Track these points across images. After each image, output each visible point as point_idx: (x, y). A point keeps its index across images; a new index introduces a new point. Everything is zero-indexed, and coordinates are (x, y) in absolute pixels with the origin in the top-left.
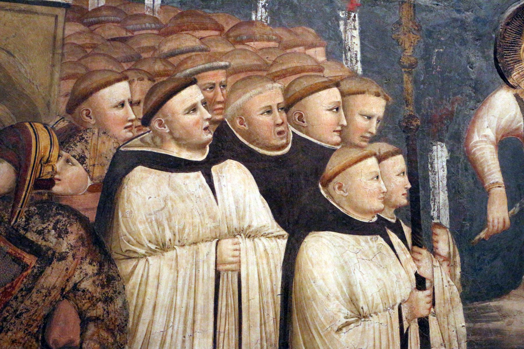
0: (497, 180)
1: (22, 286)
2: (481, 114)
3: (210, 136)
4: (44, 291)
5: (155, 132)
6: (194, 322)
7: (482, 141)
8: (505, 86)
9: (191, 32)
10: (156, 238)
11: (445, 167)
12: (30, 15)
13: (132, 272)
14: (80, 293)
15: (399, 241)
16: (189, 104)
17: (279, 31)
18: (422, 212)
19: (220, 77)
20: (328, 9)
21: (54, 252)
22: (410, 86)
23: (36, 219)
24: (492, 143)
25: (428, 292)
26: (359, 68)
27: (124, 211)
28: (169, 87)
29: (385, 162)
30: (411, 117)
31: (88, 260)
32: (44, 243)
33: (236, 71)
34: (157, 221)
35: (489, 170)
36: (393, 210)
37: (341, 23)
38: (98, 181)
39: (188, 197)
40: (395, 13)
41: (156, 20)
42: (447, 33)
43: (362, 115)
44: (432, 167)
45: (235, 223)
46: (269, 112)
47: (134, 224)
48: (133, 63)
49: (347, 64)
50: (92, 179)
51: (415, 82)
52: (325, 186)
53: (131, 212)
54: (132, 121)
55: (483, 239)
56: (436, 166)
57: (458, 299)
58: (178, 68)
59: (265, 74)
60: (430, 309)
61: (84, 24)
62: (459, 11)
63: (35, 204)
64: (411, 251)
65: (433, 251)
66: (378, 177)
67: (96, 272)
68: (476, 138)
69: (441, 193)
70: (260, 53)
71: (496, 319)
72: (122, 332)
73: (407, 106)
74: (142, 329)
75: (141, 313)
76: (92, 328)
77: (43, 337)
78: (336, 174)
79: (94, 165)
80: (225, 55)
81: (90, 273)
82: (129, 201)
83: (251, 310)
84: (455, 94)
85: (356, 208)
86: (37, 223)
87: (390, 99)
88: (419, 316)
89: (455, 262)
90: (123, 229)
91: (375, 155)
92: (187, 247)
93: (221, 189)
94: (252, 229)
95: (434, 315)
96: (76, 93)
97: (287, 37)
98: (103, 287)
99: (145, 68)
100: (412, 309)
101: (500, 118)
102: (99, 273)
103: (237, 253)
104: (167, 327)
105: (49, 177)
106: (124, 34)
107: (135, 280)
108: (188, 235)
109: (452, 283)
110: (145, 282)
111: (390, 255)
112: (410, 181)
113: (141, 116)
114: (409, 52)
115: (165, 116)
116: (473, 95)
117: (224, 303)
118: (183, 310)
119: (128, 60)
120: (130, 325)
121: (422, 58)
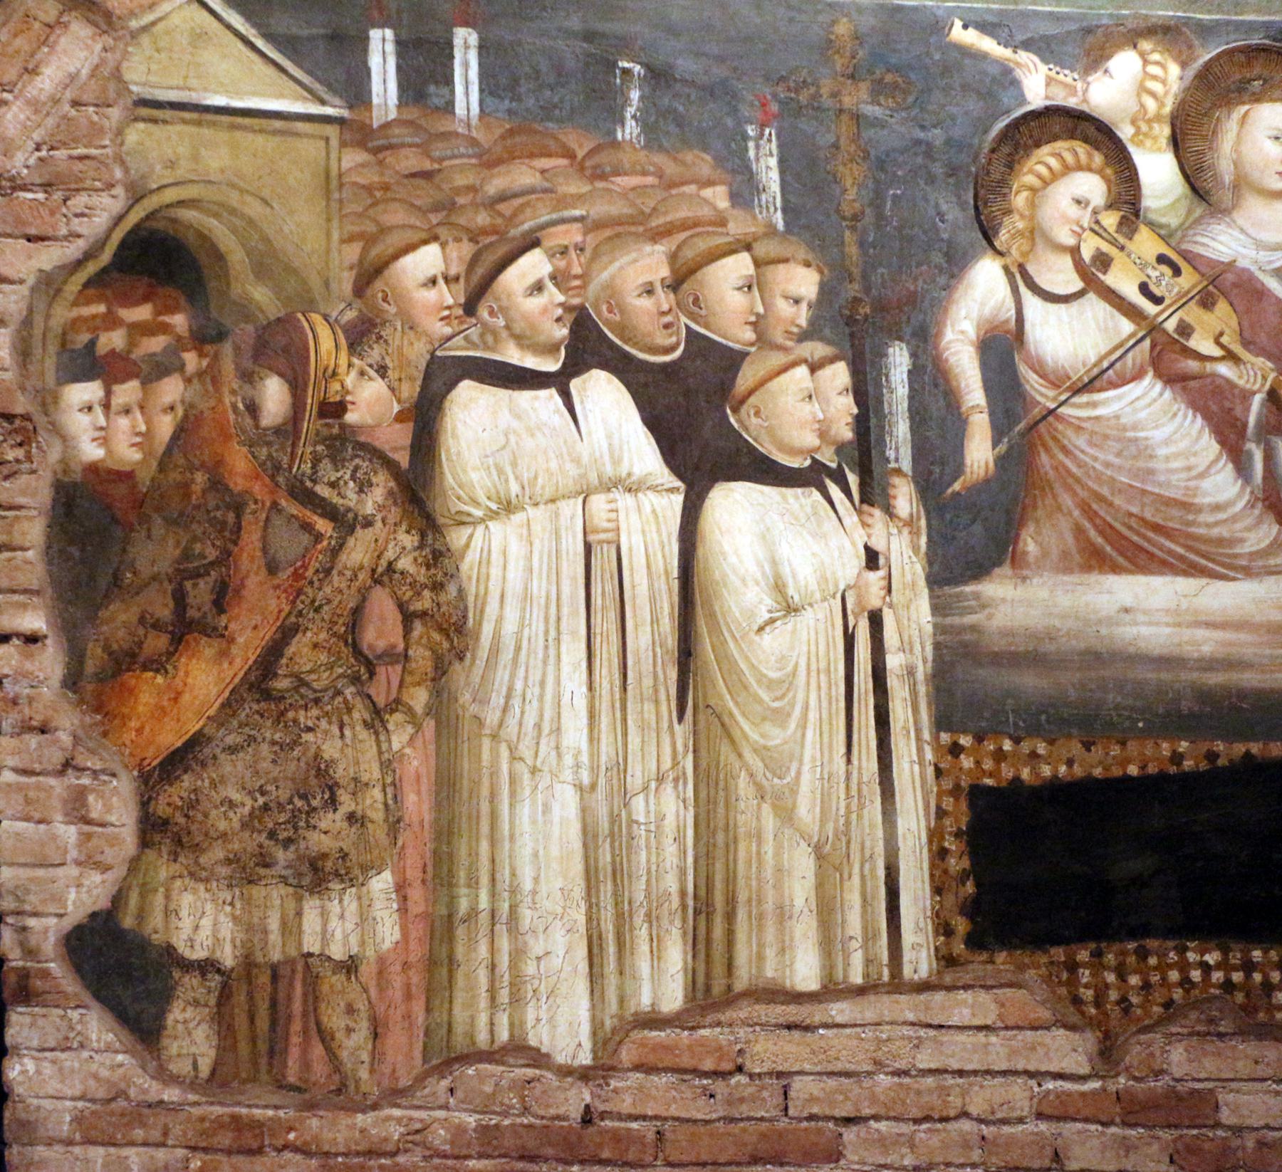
0: (977, 402)
1: (317, 565)
2: (956, 296)
3: (565, 332)
4: (348, 573)
5: (485, 325)
6: (559, 619)
8: (990, 252)
9: (527, 161)
10: (498, 492)
11: (906, 380)
12: (289, 139)
13: (467, 545)
14: (397, 576)
15: (843, 496)
16: (531, 280)
17: (659, 159)
18: (873, 452)
19: (573, 235)
20: (729, 122)
21: (356, 515)
22: (853, 250)
23: (326, 465)
24: (972, 343)
25: (882, 573)
26: (779, 220)
27: (448, 451)
28: (501, 251)
29: (820, 373)
30: (856, 301)
31: (404, 527)
32: (341, 501)
33: (598, 225)
34: (497, 466)
35: (967, 386)
36: (833, 449)
37: (751, 144)
38: (407, 405)
39: (539, 429)
41: (474, 142)
42: (906, 163)
43: (786, 298)
44: (887, 380)
45: (609, 470)
46: (650, 292)
47: (465, 471)
48: (444, 213)
49: (761, 213)
50: (399, 401)
51: (862, 244)
52: (735, 410)
53: (459, 453)
54: (449, 308)
55: (958, 494)
56: (893, 379)
57: (922, 583)
58: (512, 219)
59: (641, 229)
61: (367, 150)
62: (923, 127)
63: (323, 441)
64: (859, 512)
65: (889, 511)
66: (810, 397)
67: (416, 544)
68: (949, 335)
69: (901, 421)
70: (631, 196)
71: (972, 611)
72: (460, 633)
74: (487, 630)
75: (484, 604)
76: (418, 628)
77: (354, 639)
78: (751, 393)
79: (400, 380)
80: (579, 199)
81: (409, 546)
82: (454, 436)
83: (638, 602)
84: (919, 265)
85: (783, 448)
86: (327, 471)
88: (870, 608)
89: (919, 528)
90: (449, 479)
91: (806, 361)
92: (542, 507)
93: (586, 417)
94: (634, 478)
95: (891, 606)
96: (366, 265)
97: (671, 169)
98: (428, 567)
99: (462, 221)
100: (860, 599)
101: (983, 304)
102: (421, 547)
103: (613, 515)
104: (522, 626)
105: (338, 398)
106: (427, 165)
107: (471, 557)
108: (543, 488)
109: (914, 559)
110: (485, 561)
111: (829, 517)
112: (857, 403)
113: (462, 300)
114: (852, 194)
115: (497, 299)
116: (945, 265)
117: (599, 591)
118: (543, 601)
119: (436, 208)
120: (471, 622)
121: (870, 205)
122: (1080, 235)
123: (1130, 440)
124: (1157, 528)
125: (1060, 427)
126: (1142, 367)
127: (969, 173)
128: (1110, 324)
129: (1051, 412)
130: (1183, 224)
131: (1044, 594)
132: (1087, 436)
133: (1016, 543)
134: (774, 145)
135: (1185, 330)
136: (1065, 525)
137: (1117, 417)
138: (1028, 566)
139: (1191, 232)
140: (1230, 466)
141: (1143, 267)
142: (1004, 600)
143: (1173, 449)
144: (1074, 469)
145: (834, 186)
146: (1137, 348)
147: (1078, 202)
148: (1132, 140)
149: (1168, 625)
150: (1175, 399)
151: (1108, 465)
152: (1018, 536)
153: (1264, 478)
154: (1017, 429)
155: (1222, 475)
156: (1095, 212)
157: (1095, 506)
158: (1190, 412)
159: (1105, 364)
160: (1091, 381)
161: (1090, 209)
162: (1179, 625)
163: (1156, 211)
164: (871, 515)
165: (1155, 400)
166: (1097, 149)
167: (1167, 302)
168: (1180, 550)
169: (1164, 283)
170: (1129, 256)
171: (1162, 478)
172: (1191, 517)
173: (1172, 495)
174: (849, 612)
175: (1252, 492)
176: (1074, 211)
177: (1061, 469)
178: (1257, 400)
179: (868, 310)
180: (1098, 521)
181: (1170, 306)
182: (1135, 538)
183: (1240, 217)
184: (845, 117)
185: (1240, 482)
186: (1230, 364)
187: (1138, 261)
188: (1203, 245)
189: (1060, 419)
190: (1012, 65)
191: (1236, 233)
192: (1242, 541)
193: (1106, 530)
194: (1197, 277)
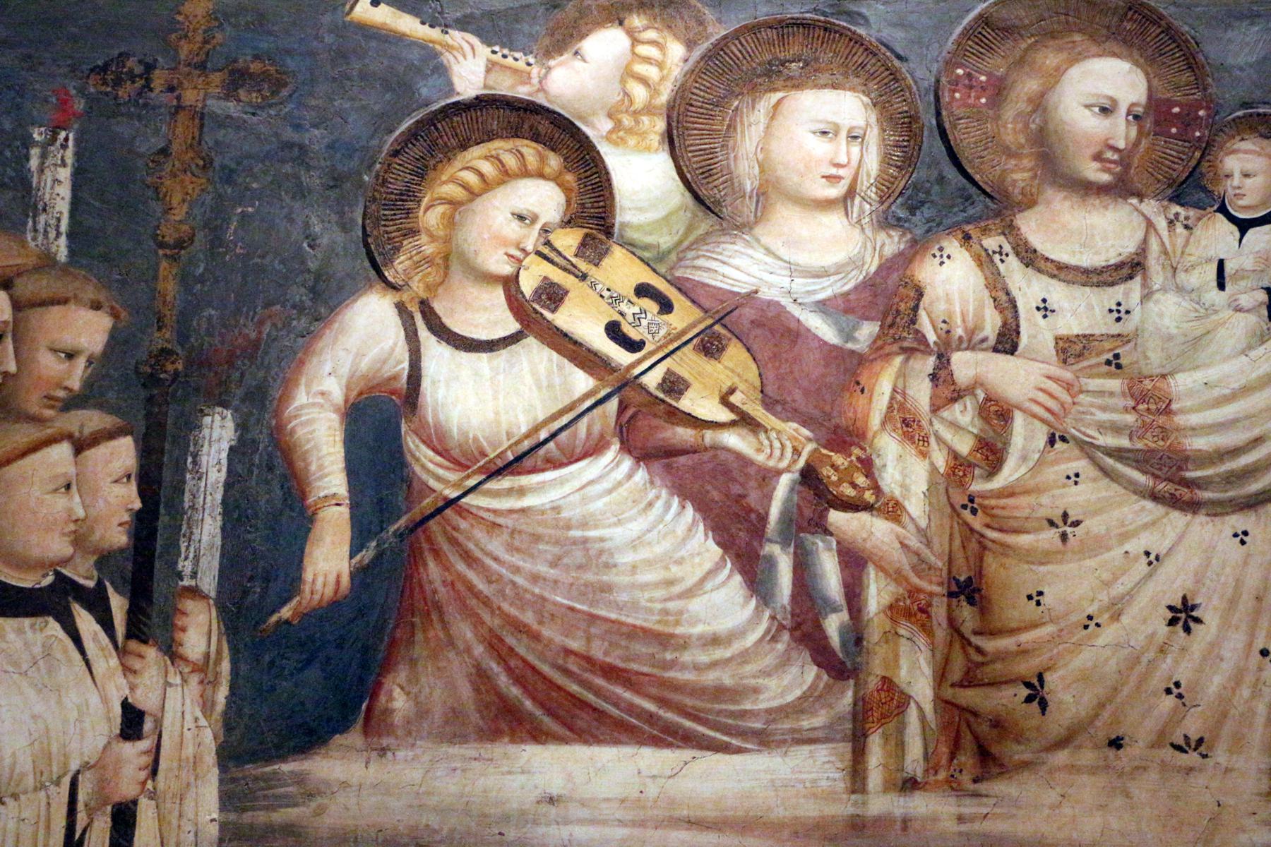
0: (334, 490)
7: (314, 404)
8: (379, 286)
11: (224, 462)
15: (98, 628)
18: (157, 564)
22: (169, 287)
24: (337, 410)
25: (145, 744)
26: (61, 249)
29: (91, 454)
30: (166, 353)
35: (321, 467)
36: (92, 559)
37: (35, 152)
40: (157, 131)
42: (265, 173)
43: (54, 351)
44: (195, 463)
49: (34, 239)
51: (185, 280)
55: (287, 622)
56: (204, 459)
57: (210, 758)
60: (144, 783)
62: (298, 127)
64: (121, 652)
65: (172, 652)
66: (68, 487)
68: (301, 397)
69: (208, 520)
73: (159, 329)
84: (268, 305)
87: (123, 315)
88: (117, 799)
89: (217, 675)
91: (69, 437)
95: (153, 795)
100: (102, 784)
101: (360, 355)
109: (203, 722)
111: (70, 661)
112: (142, 493)
114: (179, 213)
116: (308, 303)
121: (206, 225)
122: (520, 261)
123: (574, 542)
124: (611, 672)
125: (463, 525)
126: (602, 436)
127: (361, 185)
128: (557, 380)
129: (450, 503)
130: (680, 242)
131: (415, 774)
132: (506, 537)
133: (374, 695)
134: (69, 154)
135: (674, 385)
136: (458, 669)
137: (556, 509)
138: (390, 730)
139: (690, 255)
140: (738, 578)
141: (615, 300)
142: (345, 785)
143: (644, 554)
144: (481, 585)
145: (153, 204)
146: (599, 410)
147: (521, 218)
148: (608, 138)
149: (621, 823)
150: (652, 483)
151: (535, 578)
152: (379, 685)
153: (794, 597)
154: (392, 529)
155: (723, 591)
156: (545, 230)
157: (510, 640)
158: (676, 501)
159: (543, 435)
160: (519, 459)
161: (538, 226)
162: (642, 824)
163: (639, 228)
164: (141, 656)
165: (620, 484)
166: (553, 150)
167: (648, 347)
168: (650, 706)
169: (644, 322)
170: (593, 286)
171: (623, 597)
172: (669, 656)
173: (638, 623)
174: (80, 806)
175: (773, 618)
176: (513, 229)
177: (459, 586)
178: (785, 481)
179: (180, 366)
180: (513, 663)
181: (651, 353)
182: (574, 688)
183: (766, 233)
184: (181, 117)
185: (753, 602)
186: (744, 431)
187: (606, 294)
188: (708, 270)
189: (464, 512)
190: (438, 47)
191: (759, 255)
192: (756, 690)
193: (526, 675)
194: (698, 313)
